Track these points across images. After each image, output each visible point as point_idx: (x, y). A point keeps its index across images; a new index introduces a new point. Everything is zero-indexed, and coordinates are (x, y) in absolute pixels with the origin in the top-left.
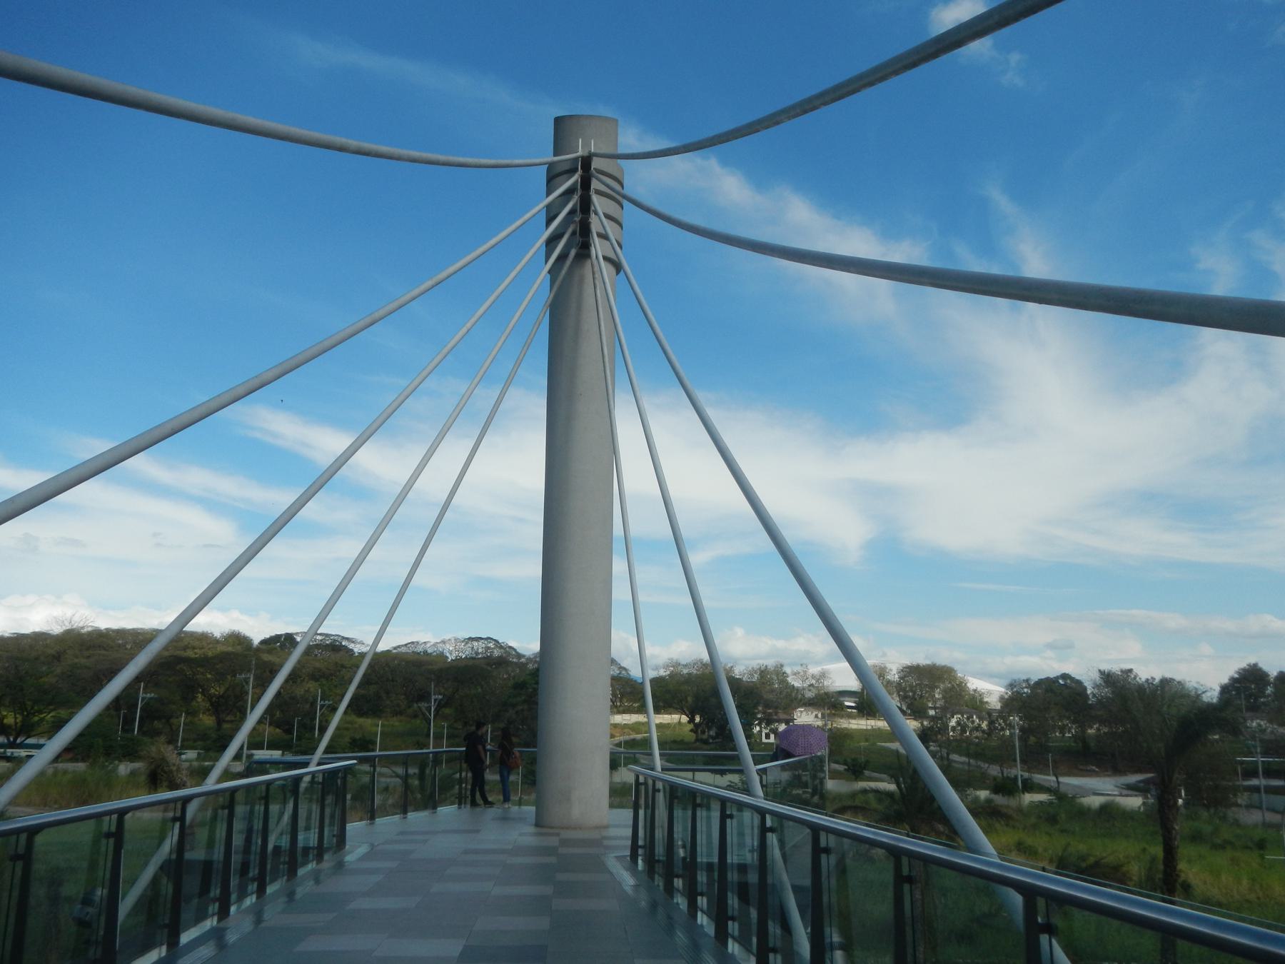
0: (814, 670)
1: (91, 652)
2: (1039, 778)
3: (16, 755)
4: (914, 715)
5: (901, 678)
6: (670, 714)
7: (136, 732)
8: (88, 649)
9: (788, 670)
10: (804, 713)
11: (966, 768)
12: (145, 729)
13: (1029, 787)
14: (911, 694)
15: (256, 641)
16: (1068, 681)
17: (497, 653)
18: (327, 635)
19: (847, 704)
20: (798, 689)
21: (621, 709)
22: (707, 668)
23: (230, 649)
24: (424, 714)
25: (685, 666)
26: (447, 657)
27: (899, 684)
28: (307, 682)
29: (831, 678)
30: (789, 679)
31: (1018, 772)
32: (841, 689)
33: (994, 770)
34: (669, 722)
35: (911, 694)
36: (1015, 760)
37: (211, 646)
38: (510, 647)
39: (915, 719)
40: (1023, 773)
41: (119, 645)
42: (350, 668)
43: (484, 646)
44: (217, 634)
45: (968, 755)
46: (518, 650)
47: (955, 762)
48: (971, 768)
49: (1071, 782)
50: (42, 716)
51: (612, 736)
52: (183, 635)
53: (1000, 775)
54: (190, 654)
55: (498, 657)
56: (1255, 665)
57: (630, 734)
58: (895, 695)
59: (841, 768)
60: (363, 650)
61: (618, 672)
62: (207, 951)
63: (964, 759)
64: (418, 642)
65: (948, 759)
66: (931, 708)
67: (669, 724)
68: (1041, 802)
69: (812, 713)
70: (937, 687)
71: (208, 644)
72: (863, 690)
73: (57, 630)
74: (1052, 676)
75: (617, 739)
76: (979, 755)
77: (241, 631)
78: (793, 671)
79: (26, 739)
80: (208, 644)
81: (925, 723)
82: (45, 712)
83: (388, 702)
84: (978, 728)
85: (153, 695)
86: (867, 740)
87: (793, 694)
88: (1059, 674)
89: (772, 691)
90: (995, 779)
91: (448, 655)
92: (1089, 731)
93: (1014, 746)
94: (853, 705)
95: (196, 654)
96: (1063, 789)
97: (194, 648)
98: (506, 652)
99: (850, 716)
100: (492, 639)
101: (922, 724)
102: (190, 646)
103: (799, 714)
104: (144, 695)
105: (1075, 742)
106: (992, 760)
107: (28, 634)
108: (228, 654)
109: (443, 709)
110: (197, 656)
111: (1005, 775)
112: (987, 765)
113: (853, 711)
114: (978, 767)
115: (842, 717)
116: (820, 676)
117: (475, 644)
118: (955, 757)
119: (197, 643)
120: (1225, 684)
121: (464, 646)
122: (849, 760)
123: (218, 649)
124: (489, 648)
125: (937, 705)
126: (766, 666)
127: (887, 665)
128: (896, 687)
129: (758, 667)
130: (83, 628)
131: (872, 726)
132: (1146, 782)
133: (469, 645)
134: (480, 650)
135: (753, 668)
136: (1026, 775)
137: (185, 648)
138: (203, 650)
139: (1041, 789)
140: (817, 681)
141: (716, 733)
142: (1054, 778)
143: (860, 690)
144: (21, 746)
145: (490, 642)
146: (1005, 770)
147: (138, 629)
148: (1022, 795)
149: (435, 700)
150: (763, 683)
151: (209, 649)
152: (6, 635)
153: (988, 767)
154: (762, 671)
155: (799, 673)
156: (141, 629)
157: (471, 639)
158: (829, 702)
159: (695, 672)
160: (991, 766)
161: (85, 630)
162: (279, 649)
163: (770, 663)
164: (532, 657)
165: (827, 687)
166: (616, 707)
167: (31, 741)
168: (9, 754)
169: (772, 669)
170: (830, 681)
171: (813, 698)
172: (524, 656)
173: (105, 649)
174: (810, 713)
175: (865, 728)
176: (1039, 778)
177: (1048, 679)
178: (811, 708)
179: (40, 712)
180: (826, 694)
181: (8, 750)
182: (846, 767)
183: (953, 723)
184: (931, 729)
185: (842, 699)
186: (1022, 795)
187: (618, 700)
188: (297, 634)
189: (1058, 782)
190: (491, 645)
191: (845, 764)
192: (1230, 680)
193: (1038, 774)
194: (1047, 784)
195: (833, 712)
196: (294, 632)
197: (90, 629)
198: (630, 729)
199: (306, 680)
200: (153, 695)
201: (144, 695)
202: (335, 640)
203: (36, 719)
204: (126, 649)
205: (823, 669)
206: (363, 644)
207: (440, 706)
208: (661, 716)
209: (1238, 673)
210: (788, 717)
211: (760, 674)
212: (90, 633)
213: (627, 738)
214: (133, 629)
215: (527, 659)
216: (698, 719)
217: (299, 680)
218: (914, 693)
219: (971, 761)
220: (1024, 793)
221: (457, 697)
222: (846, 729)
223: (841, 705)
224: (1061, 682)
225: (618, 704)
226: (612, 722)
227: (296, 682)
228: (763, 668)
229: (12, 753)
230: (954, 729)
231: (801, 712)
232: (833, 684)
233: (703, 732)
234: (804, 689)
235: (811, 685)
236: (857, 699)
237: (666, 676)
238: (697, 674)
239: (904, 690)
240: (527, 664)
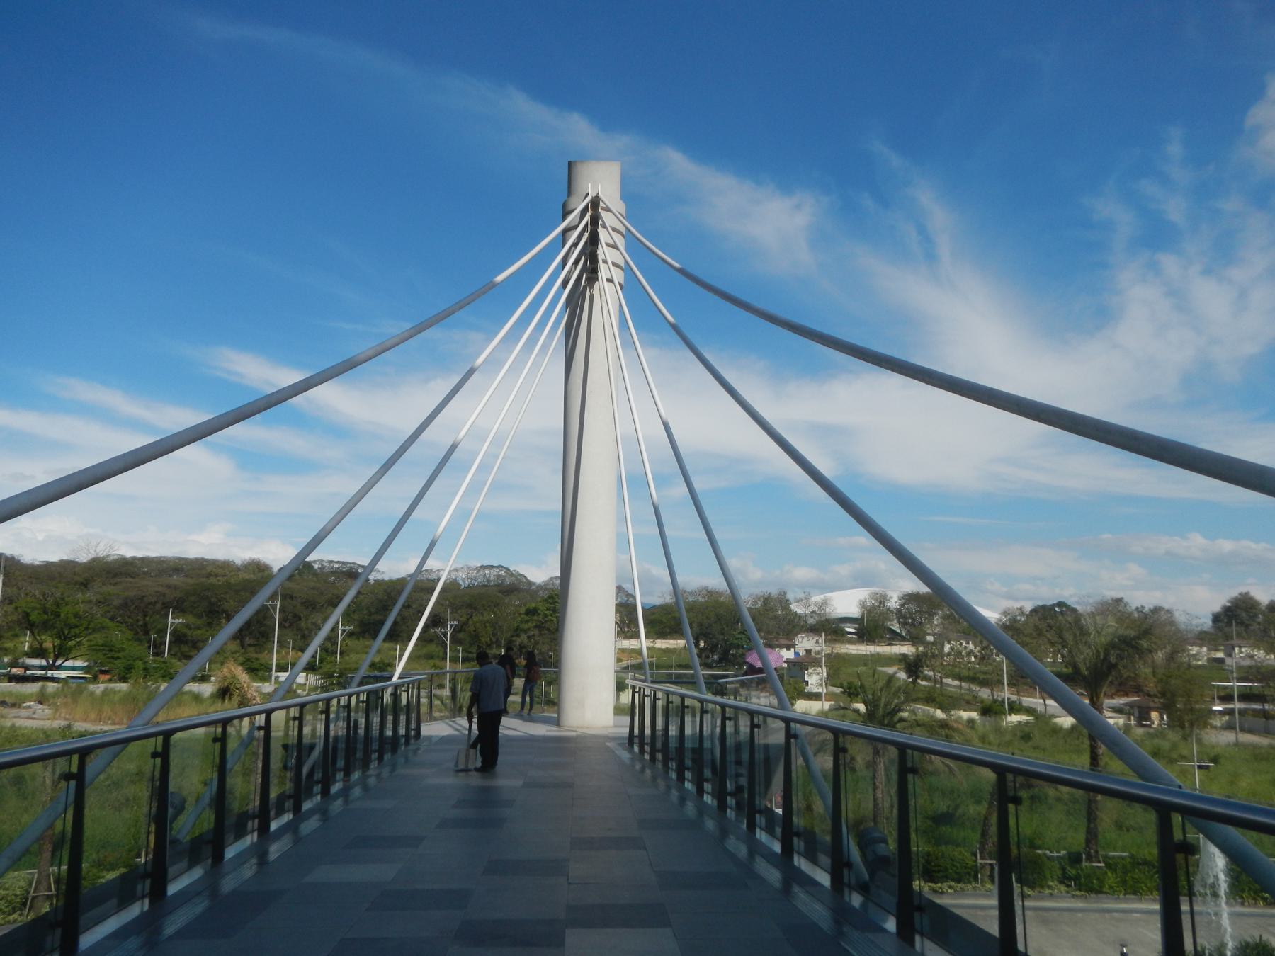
0: (817, 598)
1: (119, 580)
2: (1028, 701)
3: (55, 676)
4: (912, 641)
5: (902, 605)
6: (675, 639)
7: (166, 655)
8: (115, 575)
9: (790, 596)
10: (806, 639)
11: (959, 691)
12: (173, 653)
13: (1015, 708)
14: (910, 621)
15: (275, 570)
16: (1064, 609)
17: (508, 581)
18: (343, 563)
19: (848, 630)
20: (800, 616)
21: (628, 634)
22: (712, 595)
23: (252, 576)
24: (438, 637)
25: (691, 593)
26: (460, 585)
27: (899, 613)
28: (326, 608)
29: (832, 605)
30: (792, 607)
31: (1006, 694)
32: (840, 616)
33: (985, 693)
34: (676, 647)
35: (910, 621)
36: (1004, 684)
37: (233, 573)
38: (521, 575)
39: (913, 645)
41: (144, 573)
42: (367, 594)
43: (495, 573)
44: (238, 562)
45: (960, 678)
46: (529, 578)
47: (949, 685)
48: (963, 692)
50: (78, 640)
51: (619, 660)
52: (205, 563)
53: (991, 697)
54: (213, 580)
55: (510, 585)
57: (637, 659)
58: (895, 621)
59: (838, 690)
60: (379, 578)
61: (626, 599)
62: (249, 871)
63: (956, 683)
64: (431, 570)
65: (942, 682)
66: (930, 634)
67: (674, 649)
69: (813, 639)
70: (935, 614)
71: (230, 572)
72: (863, 616)
73: (83, 558)
74: (1049, 603)
75: (624, 664)
76: (972, 679)
77: (261, 559)
78: (795, 598)
79: (64, 662)
80: (230, 572)
81: (921, 649)
82: (82, 636)
83: (404, 627)
84: (970, 653)
85: (181, 620)
86: (865, 665)
87: (796, 621)
88: (1055, 602)
89: (776, 617)
90: (982, 702)
91: (461, 582)
93: (1003, 671)
94: (853, 630)
95: (219, 581)
97: (217, 576)
98: (517, 579)
99: (851, 642)
100: (502, 567)
101: (917, 649)
102: (213, 574)
103: (800, 640)
104: (173, 621)
105: (1066, 667)
106: (984, 683)
107: (56, 562)
108: (249, 581)
109: (458, 634)
110: (220, 583)
111: (995, 697)
112: (978, 689)
113: (854, 636)
114: (970, 690)
115: (843, 642)
116: (822, 604)
117: (487, 572)
118: (949, 681)
119: (220, 571)
120: (1217, 613)
121: (477, 573)
122: (845, 684)
123: (240, 576)
124: (499, 576)
125: (936, 631)
126: (769, 593)
127: (887, 593)
128: (896, 614)
129: (762, 594)
130: (108, 556)
131: (870, 652)
132: (1131, 705)
133: (481, 573)
134: (492, 578)
135: (757, 595)
136: (1014, 698)
137: (209, 575)
138: (225, 578)
140: (820, 608)
141: (720, 658)
142: (1042, 701)
143: (860, 617)
144: (59, 668)
145: (502, 571)
146: (995, 693)
147: (161, 557)
149: (451, 626)
150: (766, 610)
151: (231, 576)
152: (37, 563)
153: (980, 690)
154: (766, 599)
155: (802, 600)
156: (164, 557)
157: (483, 567)
158: (831, 628)
159: (700, 599)
160: (982, 690)
161: (112, 558)
162: (297, 576)
163: (774, 591)
164: (542, 584)
165: (830, 613)
166: (624, 632)
167: (68, 663)
168: (49, 675)
169: (776, 596)
170: (832, 608)
171: (815, 625)
172: (534, 584)
173: (131, 577)
174: (811, 638)
175: (864, 653)
176: (1028, 701)
177: (1044, 607)
178: (812, 634)
179: (76, 636)
180: (827, 620)
181: (49, 672)
182: (842, 690)
183: (947, 648)
184: (925, 654)
185: (843, 625)
187: (625, 625)
188: (315, 562)
189: (1045, 705)
190: (502, 573)
191: (841, 686)
192: (1222, 608)
193: (1028, 697)
195: (834, 637)
196: (312, 560)
197: (116, 557)
198: (637, 653)
199: (325, 606)
200: (181, 620)
201: (173, 621)
202: (351, 568)
203: (72, 643)
204: (151, 576)
205: (825, 597)
206: (379, 571)
207: (457, 630)
208: (667, 641)
209: (1229, 601)
210: (790, 643)
211: (764, 602)
212: (116, 561)
213: (635, 662)
214: (156, 557)
215: (538, 587)
216: (702, 645)
217: (319, 606)
218: (914, 620)
219: (963, 684)
220: (1010, 714)
221: (470, 622)
222: (846, 654)
223: (842, 631)
224: (1057, 609)
225: (626, 629)
226: (620, 647)
227: (313, 608)
228: (765, 596)
229: (52, 674)
230: (949, 654)
231: (803, 637)
232: (835, 611)
233: (708, 657)
234: (806, 616)
235: (813, 612)
236: (857, 626)
237: (671, 604)
238: (701, 601)
239: (904, 617)
240: (538, 591)
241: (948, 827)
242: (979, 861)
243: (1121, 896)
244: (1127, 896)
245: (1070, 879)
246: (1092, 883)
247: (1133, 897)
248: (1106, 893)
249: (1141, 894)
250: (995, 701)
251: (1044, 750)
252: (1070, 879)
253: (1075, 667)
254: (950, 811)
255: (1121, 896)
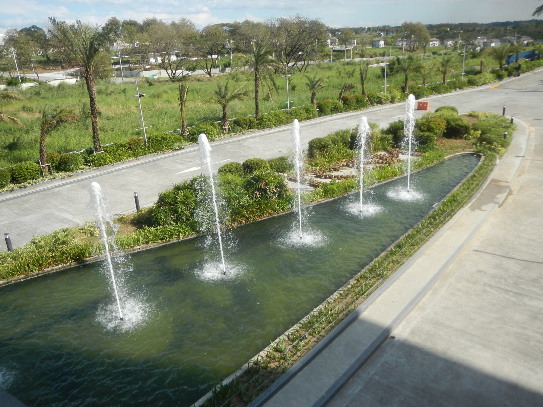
40: (21, 74)
49: (44, 76)
56: (115, 18)
68: (31, 87)
92: (49, 52)
96: (40, 79)
105: (43, 57)
139: (31, 80)
142: (36, 75)
148: (22, 85)
186: (22, 85)
193: (28, 74)
194: (33, 78)
220: (22, 83)
241: (17, 151)
242: (41, 166)
243: (115, 164)
244: (117, 163)
245: (89, 162)
246: (101, 161)
247: (119, 162)
248: (107, 164)
249: (123, 160)
250: (13, 78)
251: (48, 98)
252: (89, 162)
253: (47, 57)
254: (15, 141)
255: (115, 164)
